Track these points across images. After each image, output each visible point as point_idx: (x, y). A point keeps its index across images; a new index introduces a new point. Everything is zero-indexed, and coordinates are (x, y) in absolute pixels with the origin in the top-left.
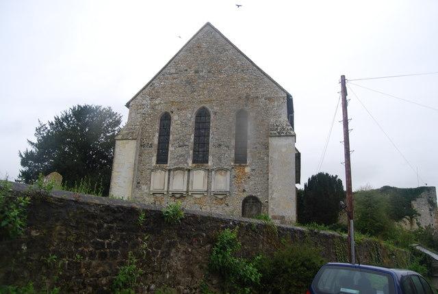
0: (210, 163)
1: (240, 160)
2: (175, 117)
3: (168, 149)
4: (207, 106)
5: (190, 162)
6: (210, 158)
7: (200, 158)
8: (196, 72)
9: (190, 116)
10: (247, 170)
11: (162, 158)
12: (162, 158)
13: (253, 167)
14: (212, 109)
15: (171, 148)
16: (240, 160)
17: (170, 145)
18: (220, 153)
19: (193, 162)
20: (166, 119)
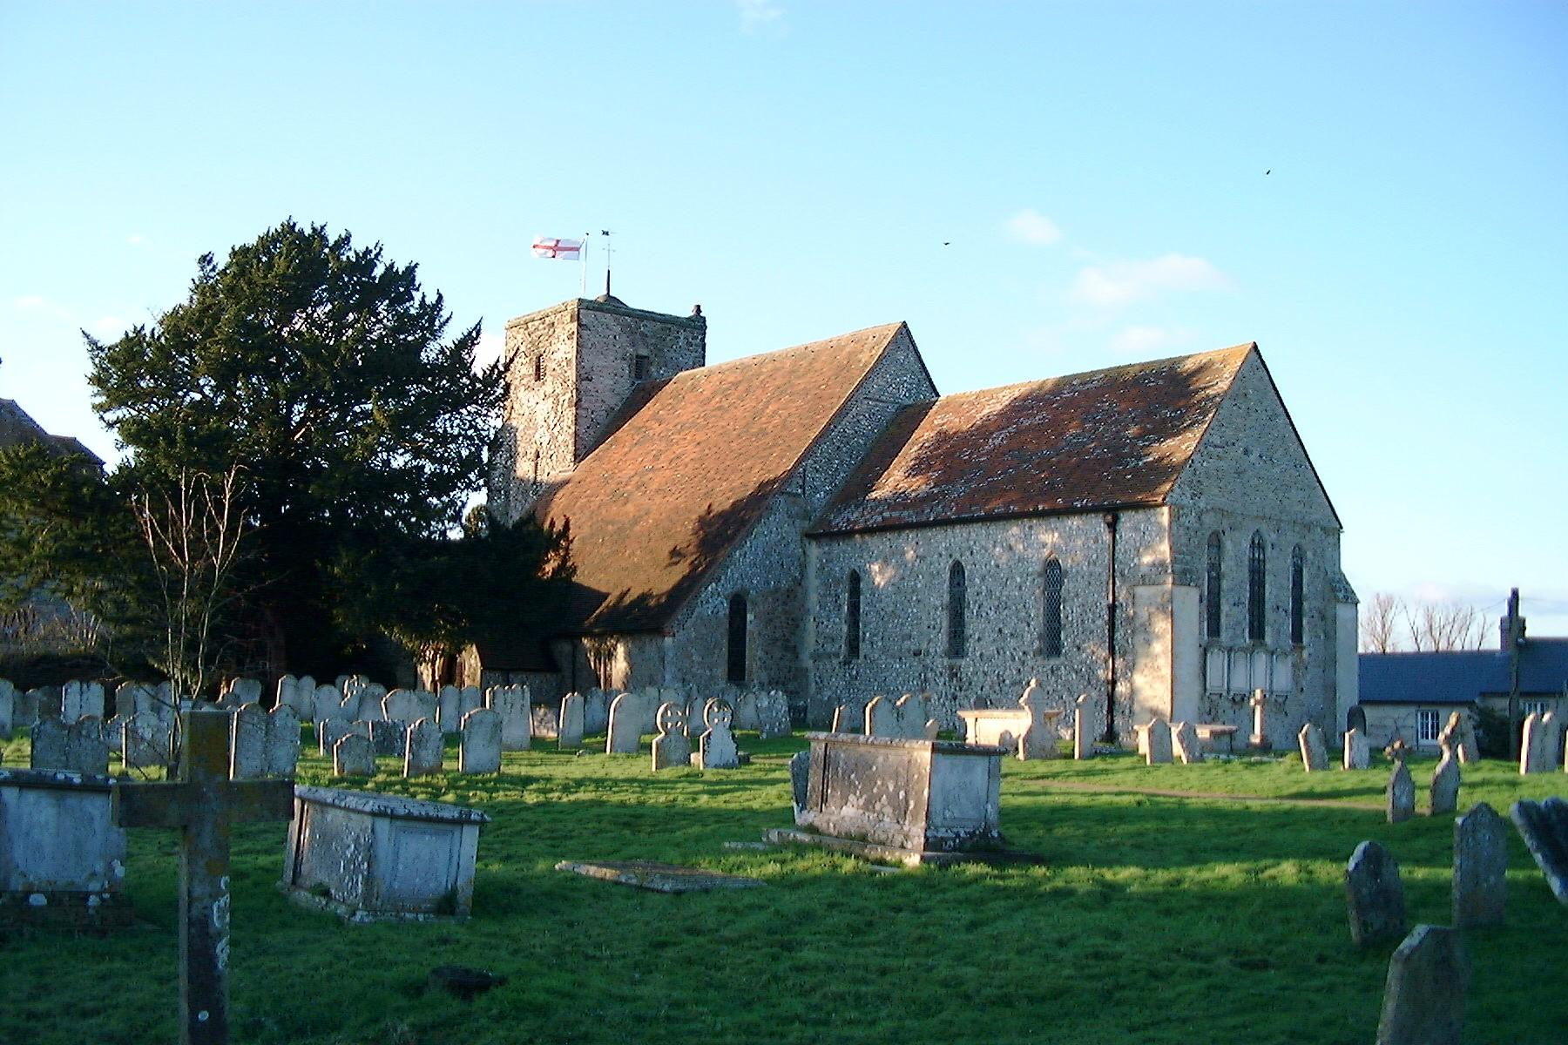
0: (1268, 640)
1: (1297, 636)
2: (1228, 545)
3: (1219, 606)
4: (1264, 527)
5: (1247, 635)
6: (1268, 629)
7: (1257, 631)
8: (1246, 452)
9: (1246, 545)
10: (1305, 654)
11: (1214, 630)
12: (1214, 630)
13: (1312, 650)
14: (1270, 537)
15: (1225, 608)
16: (1297, 636)
17: (1223, 601)
18: (1278, 625)
19: (1250, 638)
20: (1216, 542)
